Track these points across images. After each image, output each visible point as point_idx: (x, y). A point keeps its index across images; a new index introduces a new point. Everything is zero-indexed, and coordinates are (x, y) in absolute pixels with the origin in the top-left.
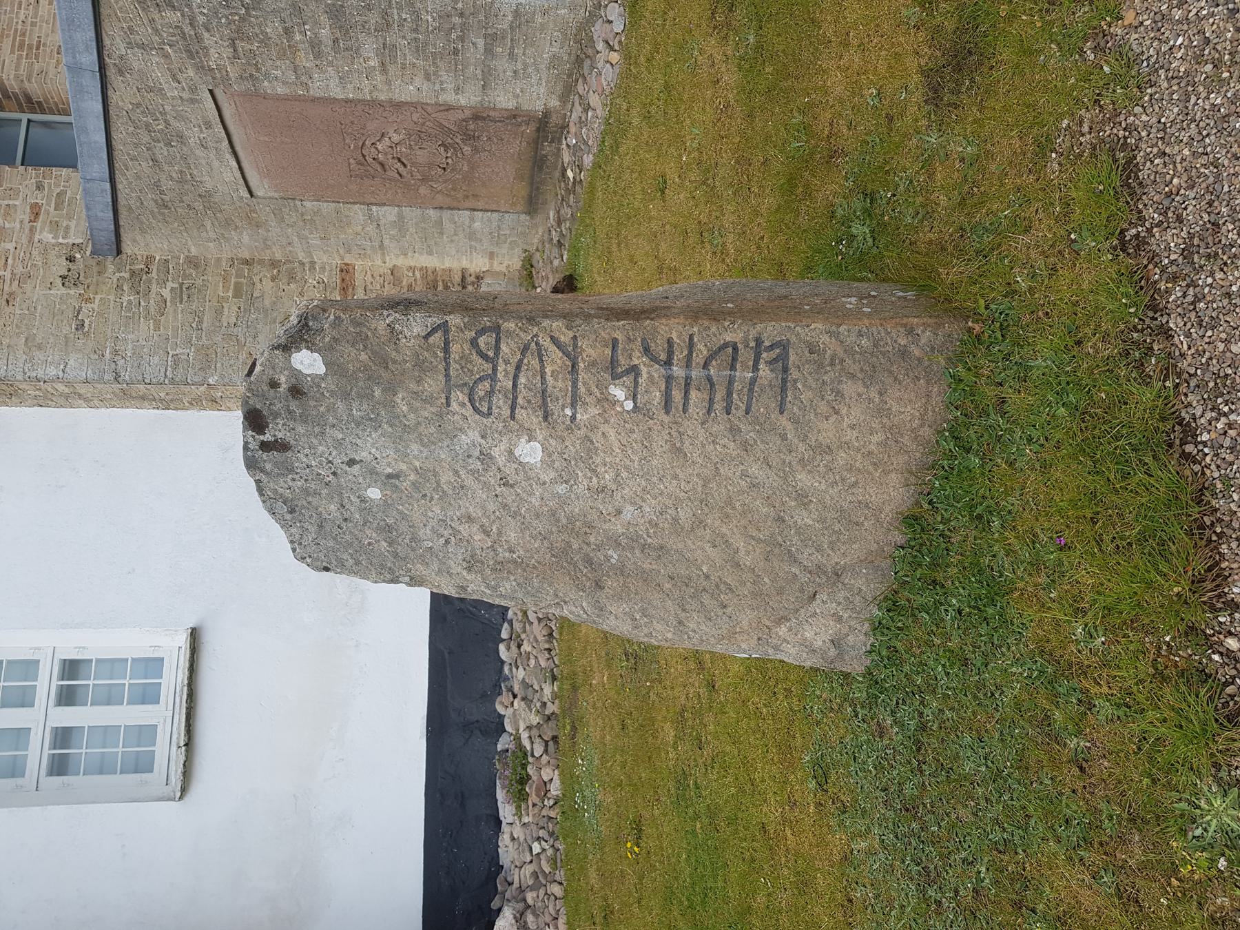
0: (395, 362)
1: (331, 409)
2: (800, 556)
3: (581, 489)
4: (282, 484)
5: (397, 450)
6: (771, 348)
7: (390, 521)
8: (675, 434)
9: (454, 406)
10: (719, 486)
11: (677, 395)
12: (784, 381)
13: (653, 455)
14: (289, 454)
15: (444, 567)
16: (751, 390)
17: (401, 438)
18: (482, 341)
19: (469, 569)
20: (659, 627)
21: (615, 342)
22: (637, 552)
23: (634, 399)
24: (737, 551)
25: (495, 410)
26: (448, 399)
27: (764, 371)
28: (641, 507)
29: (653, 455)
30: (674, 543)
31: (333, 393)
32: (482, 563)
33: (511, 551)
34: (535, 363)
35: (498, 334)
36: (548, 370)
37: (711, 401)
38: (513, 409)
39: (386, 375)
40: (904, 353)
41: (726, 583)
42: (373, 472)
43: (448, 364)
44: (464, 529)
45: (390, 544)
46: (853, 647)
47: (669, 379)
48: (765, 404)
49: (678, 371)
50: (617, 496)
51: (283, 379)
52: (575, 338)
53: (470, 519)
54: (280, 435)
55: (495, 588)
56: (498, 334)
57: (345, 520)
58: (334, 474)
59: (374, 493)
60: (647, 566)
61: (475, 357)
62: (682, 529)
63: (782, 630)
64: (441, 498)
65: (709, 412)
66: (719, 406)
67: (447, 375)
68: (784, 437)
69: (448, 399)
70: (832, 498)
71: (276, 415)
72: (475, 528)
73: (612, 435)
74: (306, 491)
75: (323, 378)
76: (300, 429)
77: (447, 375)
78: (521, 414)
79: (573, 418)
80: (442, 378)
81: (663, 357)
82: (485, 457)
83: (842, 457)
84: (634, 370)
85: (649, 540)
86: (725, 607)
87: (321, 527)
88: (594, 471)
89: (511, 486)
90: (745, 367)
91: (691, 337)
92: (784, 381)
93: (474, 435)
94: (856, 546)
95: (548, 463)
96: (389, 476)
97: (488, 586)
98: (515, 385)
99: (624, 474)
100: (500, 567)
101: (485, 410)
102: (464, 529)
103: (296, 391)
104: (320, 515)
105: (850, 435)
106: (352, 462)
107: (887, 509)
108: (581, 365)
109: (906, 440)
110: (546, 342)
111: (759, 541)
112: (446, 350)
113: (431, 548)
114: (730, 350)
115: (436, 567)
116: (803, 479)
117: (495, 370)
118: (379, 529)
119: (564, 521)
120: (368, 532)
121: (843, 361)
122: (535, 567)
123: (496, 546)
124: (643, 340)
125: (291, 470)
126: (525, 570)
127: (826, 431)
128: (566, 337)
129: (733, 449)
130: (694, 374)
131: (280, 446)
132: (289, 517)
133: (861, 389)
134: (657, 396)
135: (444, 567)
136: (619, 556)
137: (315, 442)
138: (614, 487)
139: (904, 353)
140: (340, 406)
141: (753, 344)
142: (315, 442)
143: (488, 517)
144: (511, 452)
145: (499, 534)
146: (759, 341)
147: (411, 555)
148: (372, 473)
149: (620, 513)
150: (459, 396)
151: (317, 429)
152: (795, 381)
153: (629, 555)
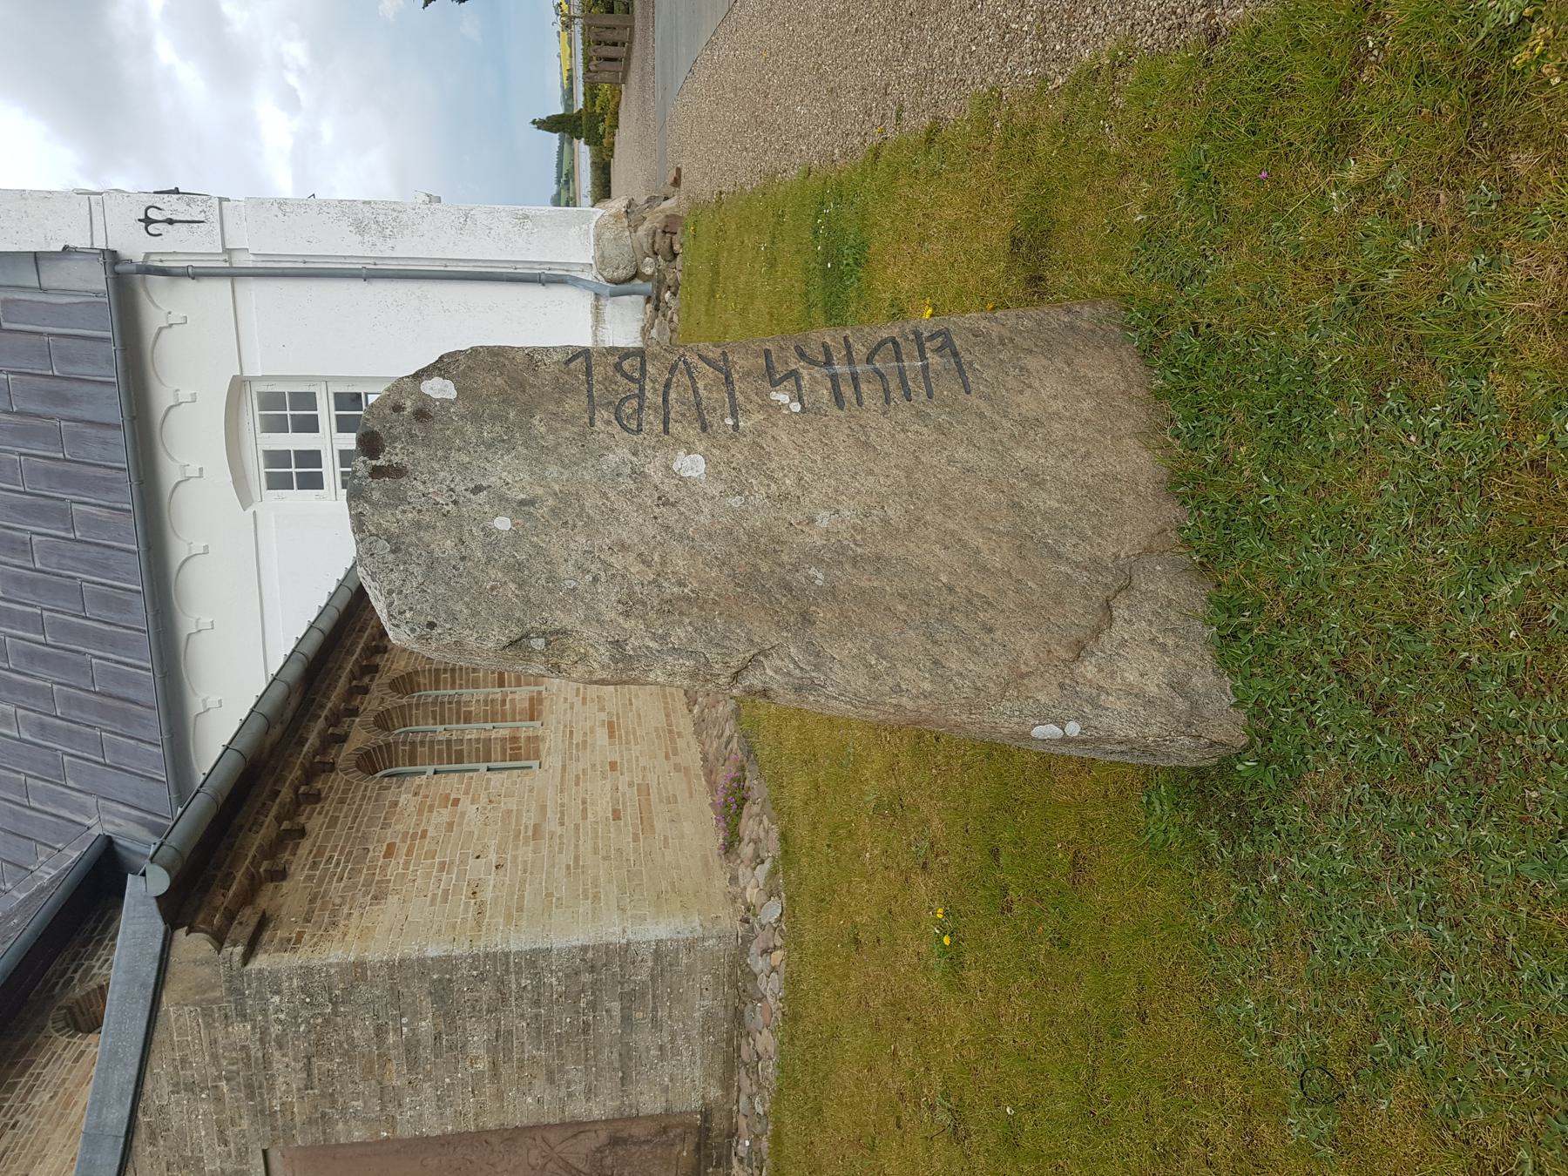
0: (533, 386)
1: (459, 432)
2: (1062, 549)
3: (759, 498)
4: (389, 517)
5: (532, 474)
6: (932, 337)
7: (521, 557)
8: (856, 428)
9: (599, 425)
10: (926, 474)
11: (847, 391)
12: (958, 364)
13: (836, 452)
14: (404, 480)
15: (592, 614)
16: (926, 378)
17: (536, 460)
18: (626, 365)
19: (627, 614)
20: (907, 673)
21: (767, 353)
22: (847, 566)
23: (800, 400)
24: (978, 551)
25: (645, 427)
26: (591, 419)
27: (933, 359)
28: (837, 511)
29: (836, 452)
30: (891, 549)
31: (462, 417)
32: (644, 604)
33: (681, 584)
34: (686, 380)
35: (643, 358)
36: (700, 385)
37: (886, 391)
38: (666, 423)
39: (523, 398)
40: (1071, 327)
41: (978, 595)
42: (502, 498)
43: (590, 385)
44: (617, 561)
45: (520, 586)
46: (1207, 695)
47: (834, 378)
48: (947, 388)
49: (841, 369)
50: (806, 501)
51: (408, 403)
52: (724, 354)
53: (624, 547)
54: (395, 459)
55: (663, 638)
56: (643, 358)
57: (463, 559)
58: (455, 502)
59: (503, 523)
60: (865, 584)
61: (619, 377)
62: (898, 530)
63: (1088, 669)
64: (586, 525)
65: (887, 401)
66: (896, 395)
67: (590, 396)
68: (981, 416)
69: (591, 419)
70: (1069, 474)
71: (395, 439)
72: (631, 557)
73: (784, 438)
74: (418, 525)
75: (452, 403)
76: (421, 453)
77: (590, 396)
78: (675, 428)
79: (736, 427)
80: (584, 398)
81: (821, 358)
82: (638, 475)
83: (1058, 430)
84: (794, 374)
85: (859, 550)
86: (991, 630)
87: (431, 567)
88: (771, 478)
89: (673, 505)
90: (912, 358)
91: (846, 339)
92: (958, 364)
93: (623, 452)
94: (1128, 528)
95: (714, 472)
96: (522, 503)
97: (654, 637)
98: (665, 400)
99: (808, 477)
100: (669, 608)
101: (634, 427)
102: (617, 561)
103: (421, 415)
104: (431, 553)
105: (1056, 406)
106: (477, 489)
107: (1142, 479)
108: (736, 376)
109: (1121, 402)
110: (693, 359)
111: (999, 534)
112: (589, 373)
113: (574, 589)
114: (890, 345)
115: (581, 613)
116: (1023, 456)
117: (642, 389)
118: (507, 568)
119: (745, 539)
120: (492, 573)
121: (1012, 340)
122: (715, 603)
123: (661, 580)
124: (797, 348)
125: (403, 500)
126: (702, 609)
127: (1027, 404)
128: (714, 354)
129: (928, 434)
130: (859, 369)
131: (396, 472)
132: (391, 557)
133: (1045, 362)
134: (825, 393)
135: (592, 614)
136: (825, 575)
137: (437, 466)
138: (799, 493)
139: (1071, 327)
140: (469, 429)
141: (912, 337)
142: (437, 466)
143: (647, 543)
144: (668, 468)
145: (663, 563)
146: (918, 335)
147: (548, 599)
148: (501, 501)
149: (814, 521)
150: (605, 413)
151: (440, 453)
152: (971, 363)
153: (839, 573)
